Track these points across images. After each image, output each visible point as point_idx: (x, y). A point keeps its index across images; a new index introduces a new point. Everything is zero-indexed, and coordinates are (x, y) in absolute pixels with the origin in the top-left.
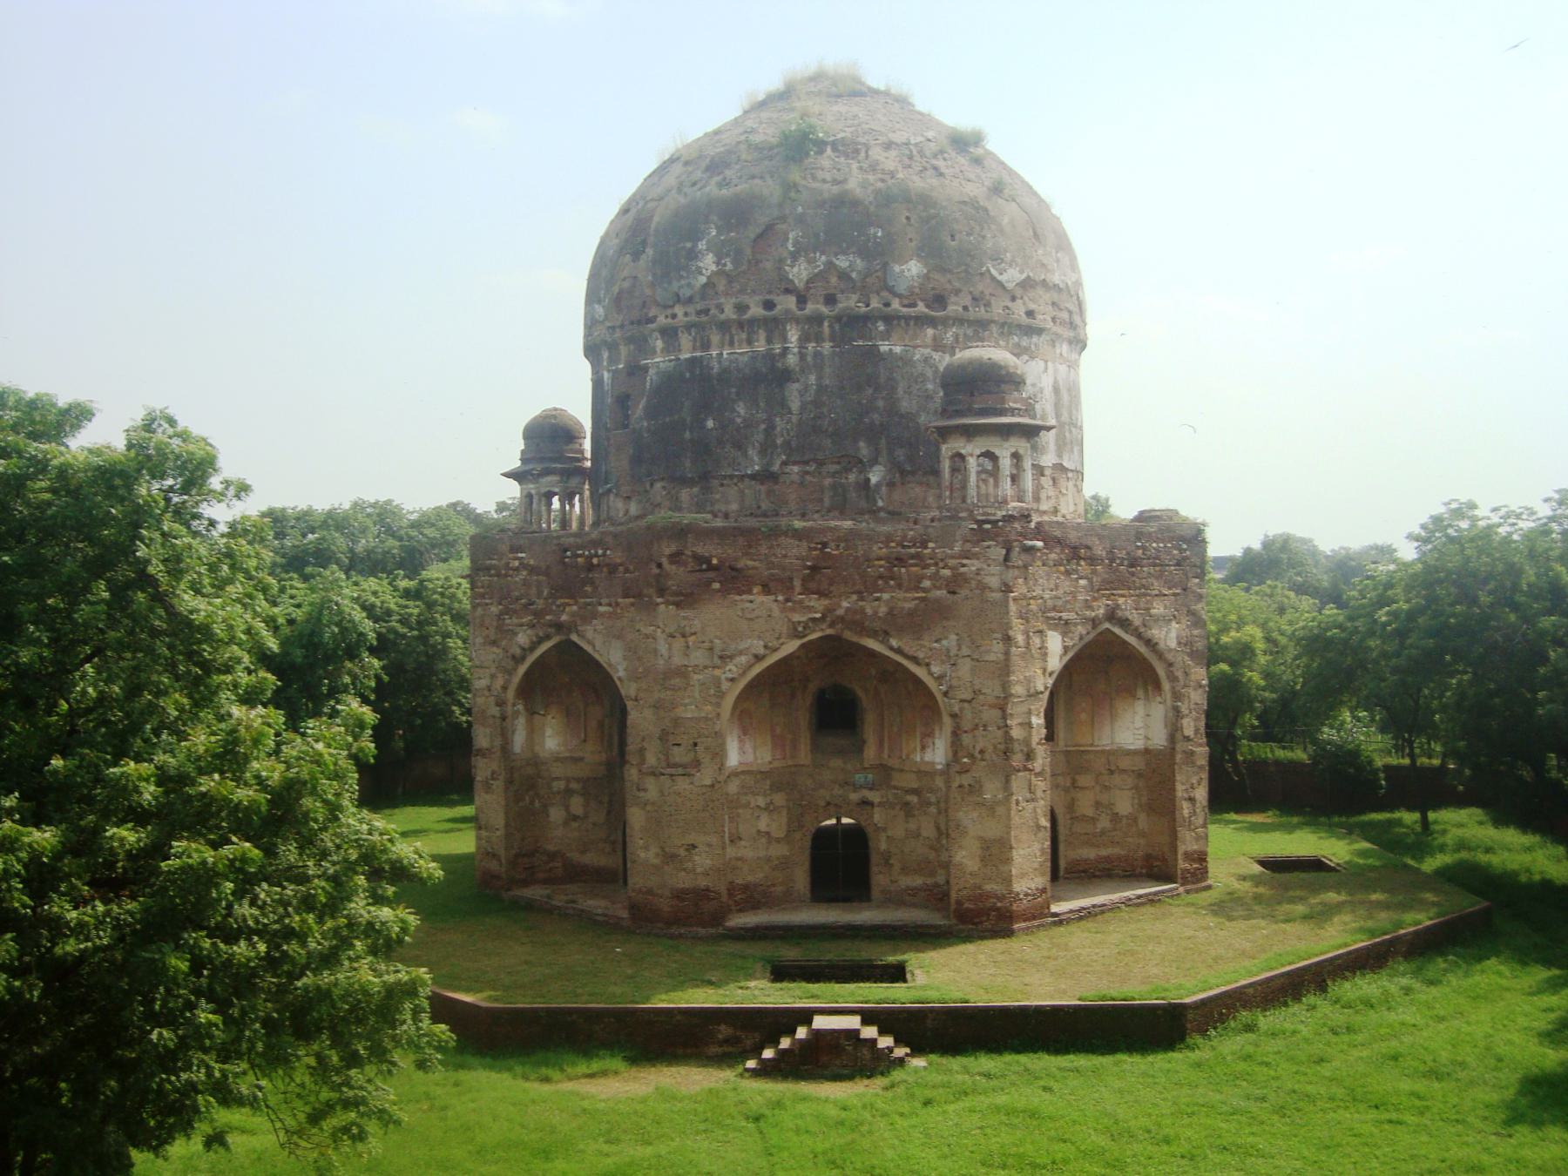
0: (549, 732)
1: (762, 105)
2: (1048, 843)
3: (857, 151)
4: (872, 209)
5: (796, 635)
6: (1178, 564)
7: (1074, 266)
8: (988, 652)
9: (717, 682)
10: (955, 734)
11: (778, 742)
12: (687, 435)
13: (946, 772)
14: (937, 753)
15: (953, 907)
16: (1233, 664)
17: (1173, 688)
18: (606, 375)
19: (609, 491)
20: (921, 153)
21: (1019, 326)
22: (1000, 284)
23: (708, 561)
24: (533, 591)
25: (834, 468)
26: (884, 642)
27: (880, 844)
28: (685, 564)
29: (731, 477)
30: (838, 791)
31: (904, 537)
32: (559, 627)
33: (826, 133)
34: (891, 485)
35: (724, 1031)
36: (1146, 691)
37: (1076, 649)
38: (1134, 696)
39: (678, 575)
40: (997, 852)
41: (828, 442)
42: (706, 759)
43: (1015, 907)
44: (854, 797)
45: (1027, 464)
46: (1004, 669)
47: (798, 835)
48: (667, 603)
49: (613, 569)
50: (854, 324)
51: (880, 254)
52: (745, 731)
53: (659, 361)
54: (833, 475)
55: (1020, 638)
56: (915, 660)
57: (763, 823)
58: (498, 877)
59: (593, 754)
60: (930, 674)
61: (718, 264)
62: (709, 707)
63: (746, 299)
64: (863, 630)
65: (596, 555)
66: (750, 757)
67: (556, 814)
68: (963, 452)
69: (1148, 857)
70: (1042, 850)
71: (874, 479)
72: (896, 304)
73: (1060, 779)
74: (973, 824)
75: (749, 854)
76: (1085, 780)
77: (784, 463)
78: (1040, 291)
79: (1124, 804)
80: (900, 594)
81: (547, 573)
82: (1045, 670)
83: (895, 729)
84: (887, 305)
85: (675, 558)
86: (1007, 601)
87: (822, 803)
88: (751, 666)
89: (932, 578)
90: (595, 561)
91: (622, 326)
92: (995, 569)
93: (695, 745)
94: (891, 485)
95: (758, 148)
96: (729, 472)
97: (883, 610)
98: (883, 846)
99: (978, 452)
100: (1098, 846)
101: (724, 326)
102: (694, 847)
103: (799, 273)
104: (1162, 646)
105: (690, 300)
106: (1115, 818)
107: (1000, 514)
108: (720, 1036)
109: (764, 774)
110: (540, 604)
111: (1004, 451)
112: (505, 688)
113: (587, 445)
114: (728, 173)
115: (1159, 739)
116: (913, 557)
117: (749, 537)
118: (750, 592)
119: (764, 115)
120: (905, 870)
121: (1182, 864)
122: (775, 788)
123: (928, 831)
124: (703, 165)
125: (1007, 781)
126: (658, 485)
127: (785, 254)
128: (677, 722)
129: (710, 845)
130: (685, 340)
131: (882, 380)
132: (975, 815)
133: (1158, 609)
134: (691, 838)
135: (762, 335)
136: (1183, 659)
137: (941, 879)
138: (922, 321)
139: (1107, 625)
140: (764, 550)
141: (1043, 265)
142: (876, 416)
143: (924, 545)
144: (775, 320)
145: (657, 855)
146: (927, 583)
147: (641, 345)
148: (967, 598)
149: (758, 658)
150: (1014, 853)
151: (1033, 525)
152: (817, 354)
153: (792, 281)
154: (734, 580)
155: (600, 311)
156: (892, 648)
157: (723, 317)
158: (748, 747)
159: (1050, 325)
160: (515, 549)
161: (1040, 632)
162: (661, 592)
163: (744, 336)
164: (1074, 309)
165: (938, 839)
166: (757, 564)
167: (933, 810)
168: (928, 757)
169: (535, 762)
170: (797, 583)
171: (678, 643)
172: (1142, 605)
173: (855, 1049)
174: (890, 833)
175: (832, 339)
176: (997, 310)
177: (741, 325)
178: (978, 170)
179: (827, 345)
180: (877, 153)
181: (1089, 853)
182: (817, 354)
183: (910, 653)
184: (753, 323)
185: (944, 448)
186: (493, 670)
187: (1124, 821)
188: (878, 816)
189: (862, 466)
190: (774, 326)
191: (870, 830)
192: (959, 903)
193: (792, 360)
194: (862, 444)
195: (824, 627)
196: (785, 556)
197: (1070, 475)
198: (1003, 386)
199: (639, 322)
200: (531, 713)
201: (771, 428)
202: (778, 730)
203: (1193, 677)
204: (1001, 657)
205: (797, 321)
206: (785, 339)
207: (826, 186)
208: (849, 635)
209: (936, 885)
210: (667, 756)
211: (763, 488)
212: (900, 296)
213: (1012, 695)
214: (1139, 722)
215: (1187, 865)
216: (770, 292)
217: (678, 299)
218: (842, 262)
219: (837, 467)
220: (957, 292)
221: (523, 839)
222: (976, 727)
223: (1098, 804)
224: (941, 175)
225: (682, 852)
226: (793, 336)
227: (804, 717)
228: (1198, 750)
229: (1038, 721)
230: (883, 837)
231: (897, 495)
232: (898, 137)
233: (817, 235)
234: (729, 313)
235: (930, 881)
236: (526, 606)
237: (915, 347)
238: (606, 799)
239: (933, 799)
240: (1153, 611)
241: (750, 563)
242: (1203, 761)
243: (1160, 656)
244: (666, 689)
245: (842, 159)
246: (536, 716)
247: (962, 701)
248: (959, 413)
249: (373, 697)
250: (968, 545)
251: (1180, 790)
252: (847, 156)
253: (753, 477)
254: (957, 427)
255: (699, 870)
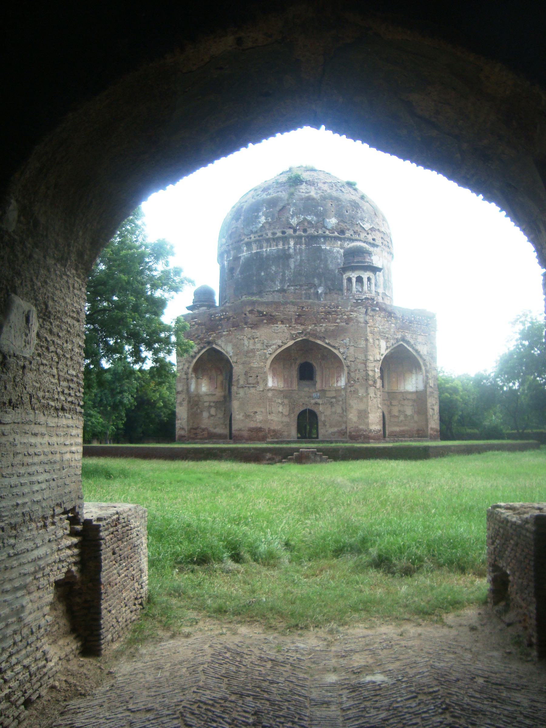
0: (203, 385)
1: (281, 174)
2: (381, 414)
3: (314, 184)
4: (319, 201)
5: (293, 339)
6: (426, 325)
7: (389, 228)
8: (360, 344)
9: (265, 354)
10: (348, 373)
11: (286, 381)
12: (255, 278)
13: (345, 389)
14: (342, 383)
15: (348, 434)
16: (450, 394)
17: (426, 369)
18: (226, 263)
19: (226, 302)
20: (336, 185)
21: (370, 243)
22: (363, 228)
23: (262, 313)
24: (200, 331)
25: (306, 287)
26: (323, 341)
27: (321, 418)
28: (254, 314)
29: (270, 291)
30: (307, 399)
31: (331, 305)
32: (209, 343)
33: (304, 179)
34: (326, 294)
35: (268, 455)
36: (416, 370)
37: (391, 348)
38: (411, 372)
39: (252, 318)
40: (363, 414)
41: (304, 279)
42: (261, 381)
43: (370, 434)
44: (313, 401)
45: (373, 281)
46: (366, 351)
47: (293, 415)
48: (248, 327)
49: (228, 319)
50: (313, 238)
51: (322, 216)
52: (274, 375)
53: (245, 254)
54: (306, 290)
55: (371, 340)
56: (334, 347)
57: (280, 409)
58: (184, 436)
59: (219, 393)
60: (340, 352)
61: (266, 220)
62: (262, 363)
63: (275, 231)
64: (316, 337)
65: (223, 315)
66: (276, 385)
67: (205, 414)
68: (351, 276)
69: (418, 430)
70: (379, 416)
71: (320, 291)
72: (327, 232)
73: (386, 402)
74: (355, 405)
75: (276, 419)
76: (394, 403)
77: (288, 286)
78: (377, 232)
79: (409, 411)
80: (330, 324)
81: (204, 325)
82: (380, 354)
83: (327, 376)
84: (324, 232)
85: (251, 312)
86: (366, 328)
87: (301, 404)
88: (276, 350)
89: (340, 319)
90: (222, 317)
91: (232, 244)
92: (362, 316)
93: (257, 376)
94: (326, 294)
95: (281, 183)
96: (269, 290)
97: (323, 330)
98: (323, 419)
99: (356, 276)
100: (400, 426)
101: (268, 240)
102: (256, 412)
103: (294, 221)
104: (421, 353)
105: (256, 232)
106: (406, 416)
107: (364, 297)
108: (267, 457)
109: (282, 392)
110: (202, 336)
111: (365, 276)
112: (188, 368)
113: (217, 298)
114: (270, 191)
115: (421, 387)
116: (333, 311)
117: (277, 304)
118: (277, 324)
119: (282, 176)
120: (331, 426)
121: (430, 432)
122: (285, 397)
123: (339, 410)
124: (261, 190)
125: (367, 389)
126: (244, 297)
127: (289, 216)
128: (251, 368)
129: (262, 412)
130: (254, 246)
131: (323, 258)
132: (356, 401)
133: (420, 339)
134: (255, 410)
135: (281, 243)
136: (427, 358)
137: (343, 427)
138: (336, 238)
139: (401, 343)
140: (282, 309)
141: (378, 224)
142: (320, 270)
143: (337, 307)
144: (286, 237)
145: (243, 416)
146: (338, 321)
147: (238, 249)
148: (352, 326)
149: (280, 347)
150: (370, 415)
151: (375, 302)
152: (300, 249)
153: (292, 224)
154: (271, 319)
155: (224, 241)
156: (326, 343)
157: (267, 237)
158: (275, 380)
159: (381, 244)
160: (193, 319)
161: (378, 339)
162: (246, 323)
163: (275, 244)
164: (390, 242)
165: (343, 413)
166: (279, 314)
167: (341, 403)
168: (339, 384)
169: (198, 396)
170: (293, 320)
171: (252, 341)
172: (414, 337)
173: (315, 457)
174: (325, 414)
175: (305, 244)
176: (363, 235)
177: (274, 240)
178: (356, 193)
179: (304, 246)
180: (320, 185)
181: (397, 429)
182: (300, 249)
183: (333, 345)
184: (279, 239)
185: (344, 276)
186: (184, 362)
187: (409, 417)
188: (321, 408)
189: (316, 287)
190: (285, 239)
191: (318, 414)
192: (350, 432)
193: (291, 251)
194: (316, 279)
195: (303, 336)
196: (289, 311)
197: (388, 298)
198: (365, 255)
199: (238, 242)
200: (197, 378)
201: (284, 274)
202: (286, 377)
203: (433, 366)
204: (364, 346)
205: (293, 237)
206: (289, 244)
207: (303, 194)
208: (312, 339)
209: (342, 430)
210: (247, 380)
211: (281, 295)
212: (329, 230)
213: (368, 359)
214: (414, 381)
215: (432, 432)
216: (284, 228)
217: (252, 232)
218: (309, 218)
219: (306, 287)
220: (349, 230)
221: (193, 423)
222: (356, 370)
223: (399, 411)
224: (343, 192)
225: (252, 414)
226: (292, 243)
227: (295, 373)
228: (435, 392)
229: (377, 370)
230: (323, 415)
231: (328, 297)
232: (328, 181)
233: (300, 209)
234: (270, 235)
235: (340, 429)
236: (197, 337)
237: (334, 247)
238: (223, 409)
239: (340, 399)
240: (418, 340)
241: (277, 314)
242: (436, 396)
243: (421, 356)
244: (247, 357)
245: (309, 186)
246: (199, 380)
247: (351, 361)
248: (349, 263)
249: (135, 396)
250: (352, 308)
251: (429, 405)
252: (311, 185)
253: (277, 291)
254: (350, 266)
255: (258, 421)
